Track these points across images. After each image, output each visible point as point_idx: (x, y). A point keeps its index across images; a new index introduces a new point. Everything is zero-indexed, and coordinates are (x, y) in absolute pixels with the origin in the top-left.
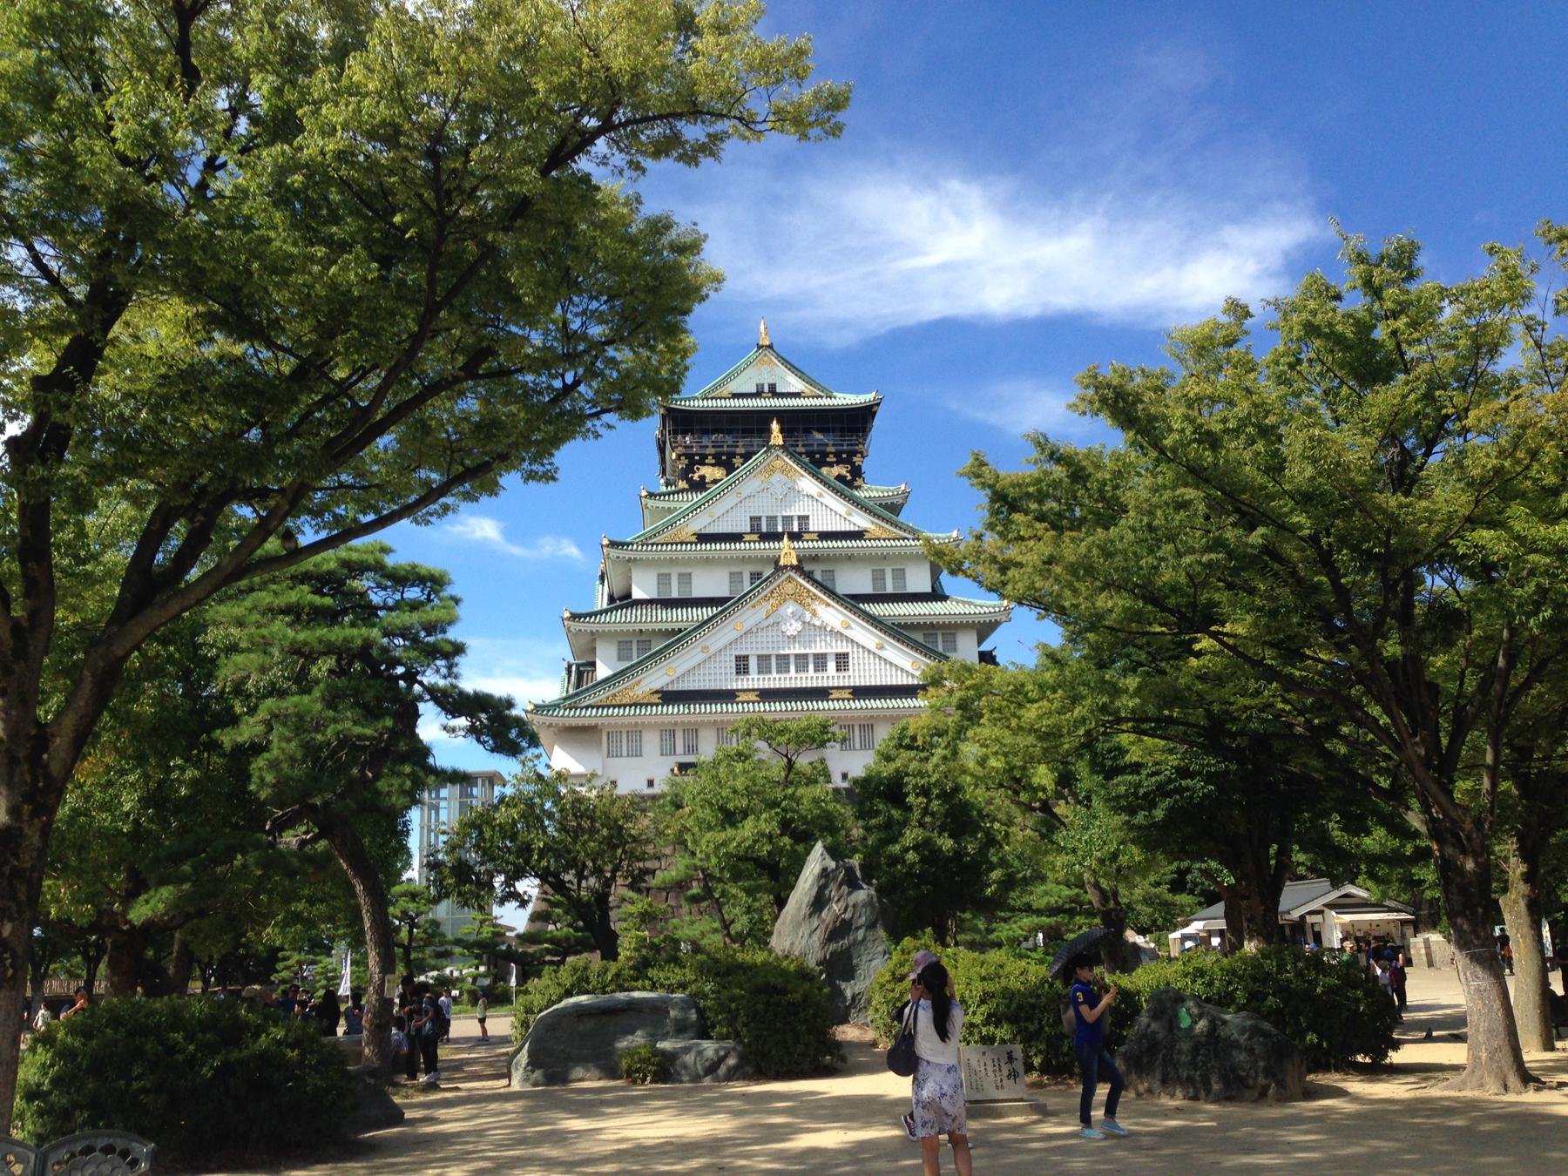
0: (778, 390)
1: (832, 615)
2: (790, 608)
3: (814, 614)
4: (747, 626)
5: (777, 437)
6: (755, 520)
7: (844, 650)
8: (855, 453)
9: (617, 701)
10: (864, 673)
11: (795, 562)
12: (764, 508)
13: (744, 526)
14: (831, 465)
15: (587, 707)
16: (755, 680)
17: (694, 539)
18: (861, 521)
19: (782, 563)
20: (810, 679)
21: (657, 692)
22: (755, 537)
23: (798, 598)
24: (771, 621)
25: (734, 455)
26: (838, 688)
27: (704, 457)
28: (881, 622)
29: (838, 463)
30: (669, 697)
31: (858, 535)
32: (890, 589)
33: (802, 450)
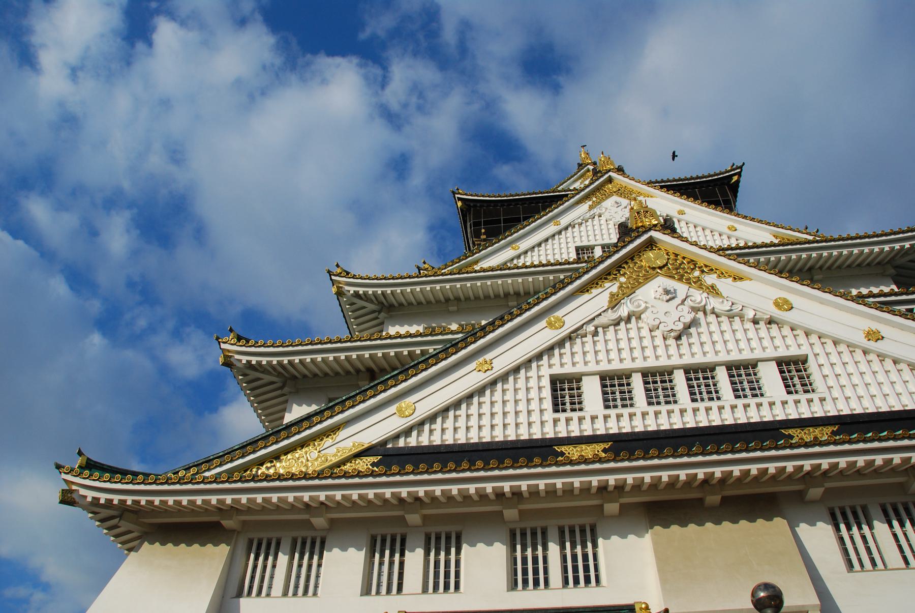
7: (793, 351)
26: (802, 423)
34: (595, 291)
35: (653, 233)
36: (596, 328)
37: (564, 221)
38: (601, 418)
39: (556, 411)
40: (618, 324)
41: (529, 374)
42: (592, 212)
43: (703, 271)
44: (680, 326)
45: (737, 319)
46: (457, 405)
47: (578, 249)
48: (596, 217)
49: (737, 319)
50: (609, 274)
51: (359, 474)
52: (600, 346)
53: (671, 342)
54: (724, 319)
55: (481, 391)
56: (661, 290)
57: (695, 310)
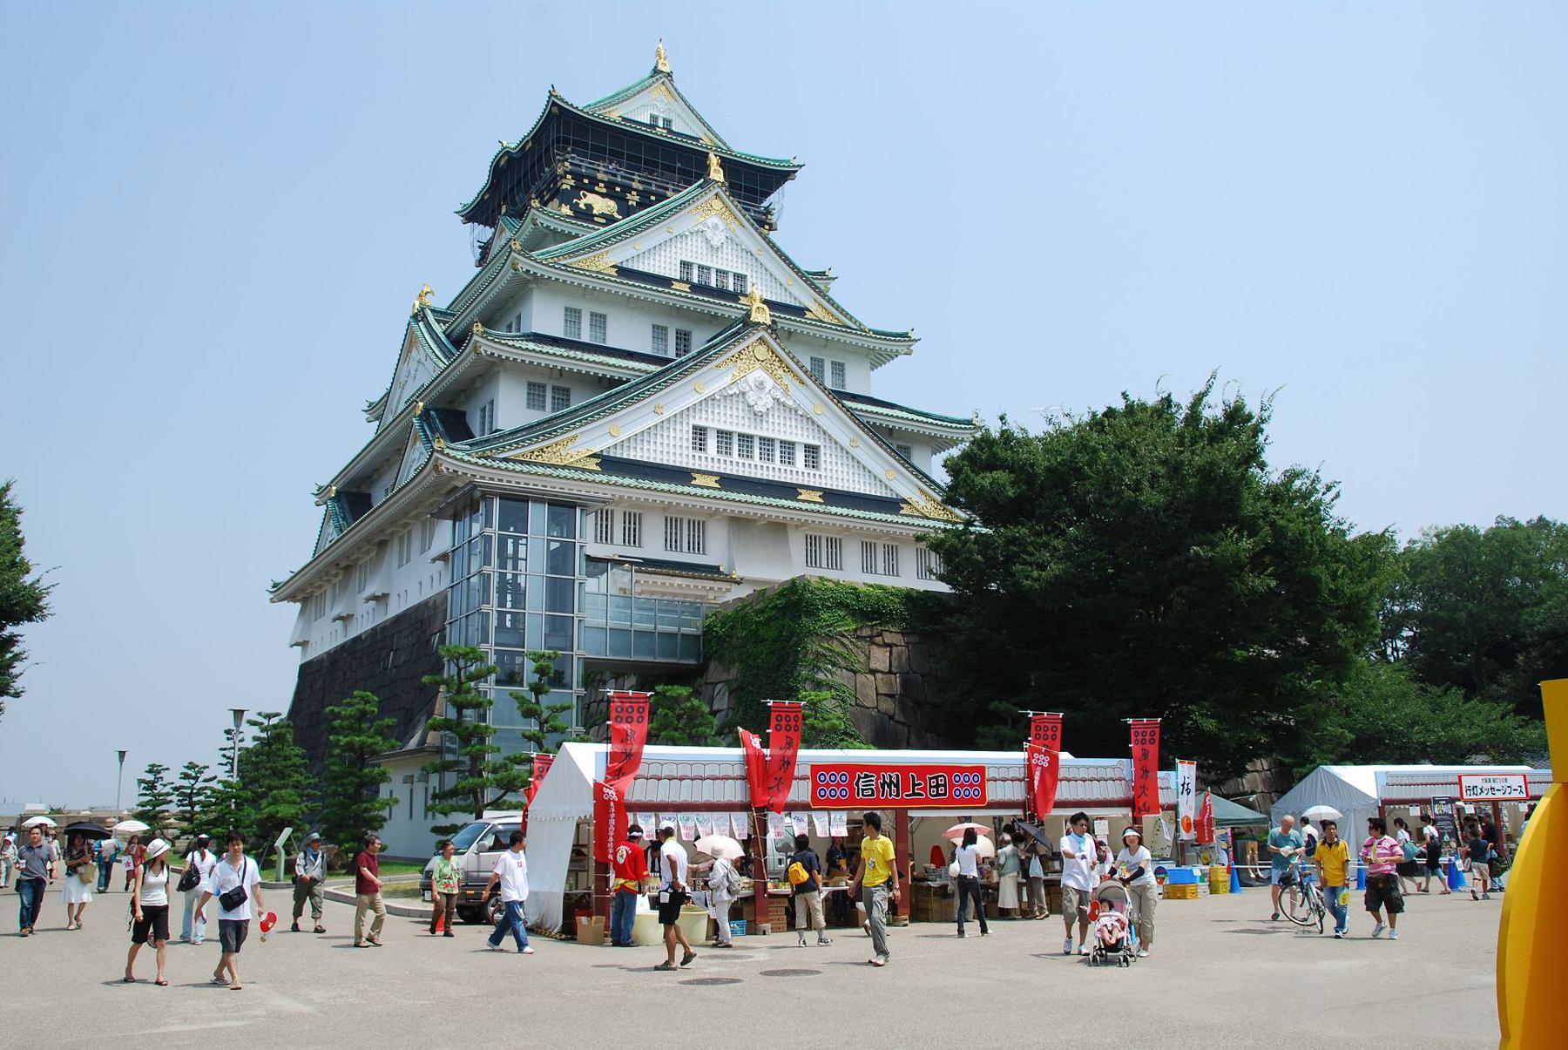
1: (807, 398)
2: (758, 374)
4: (707, 393)
6: (686, 265)
9: (545, 458)
12: (697, 254)
13: (674, 272)
15: (506, 460)
17: (613, 272)
20: (774, 471)
21: (594, 456)
22: (686, 287)
24: (735, 390)
25: (629, 189)
27: (595, 181)
30: (610, 464)
31: (800, 311)
51: (591, 472)
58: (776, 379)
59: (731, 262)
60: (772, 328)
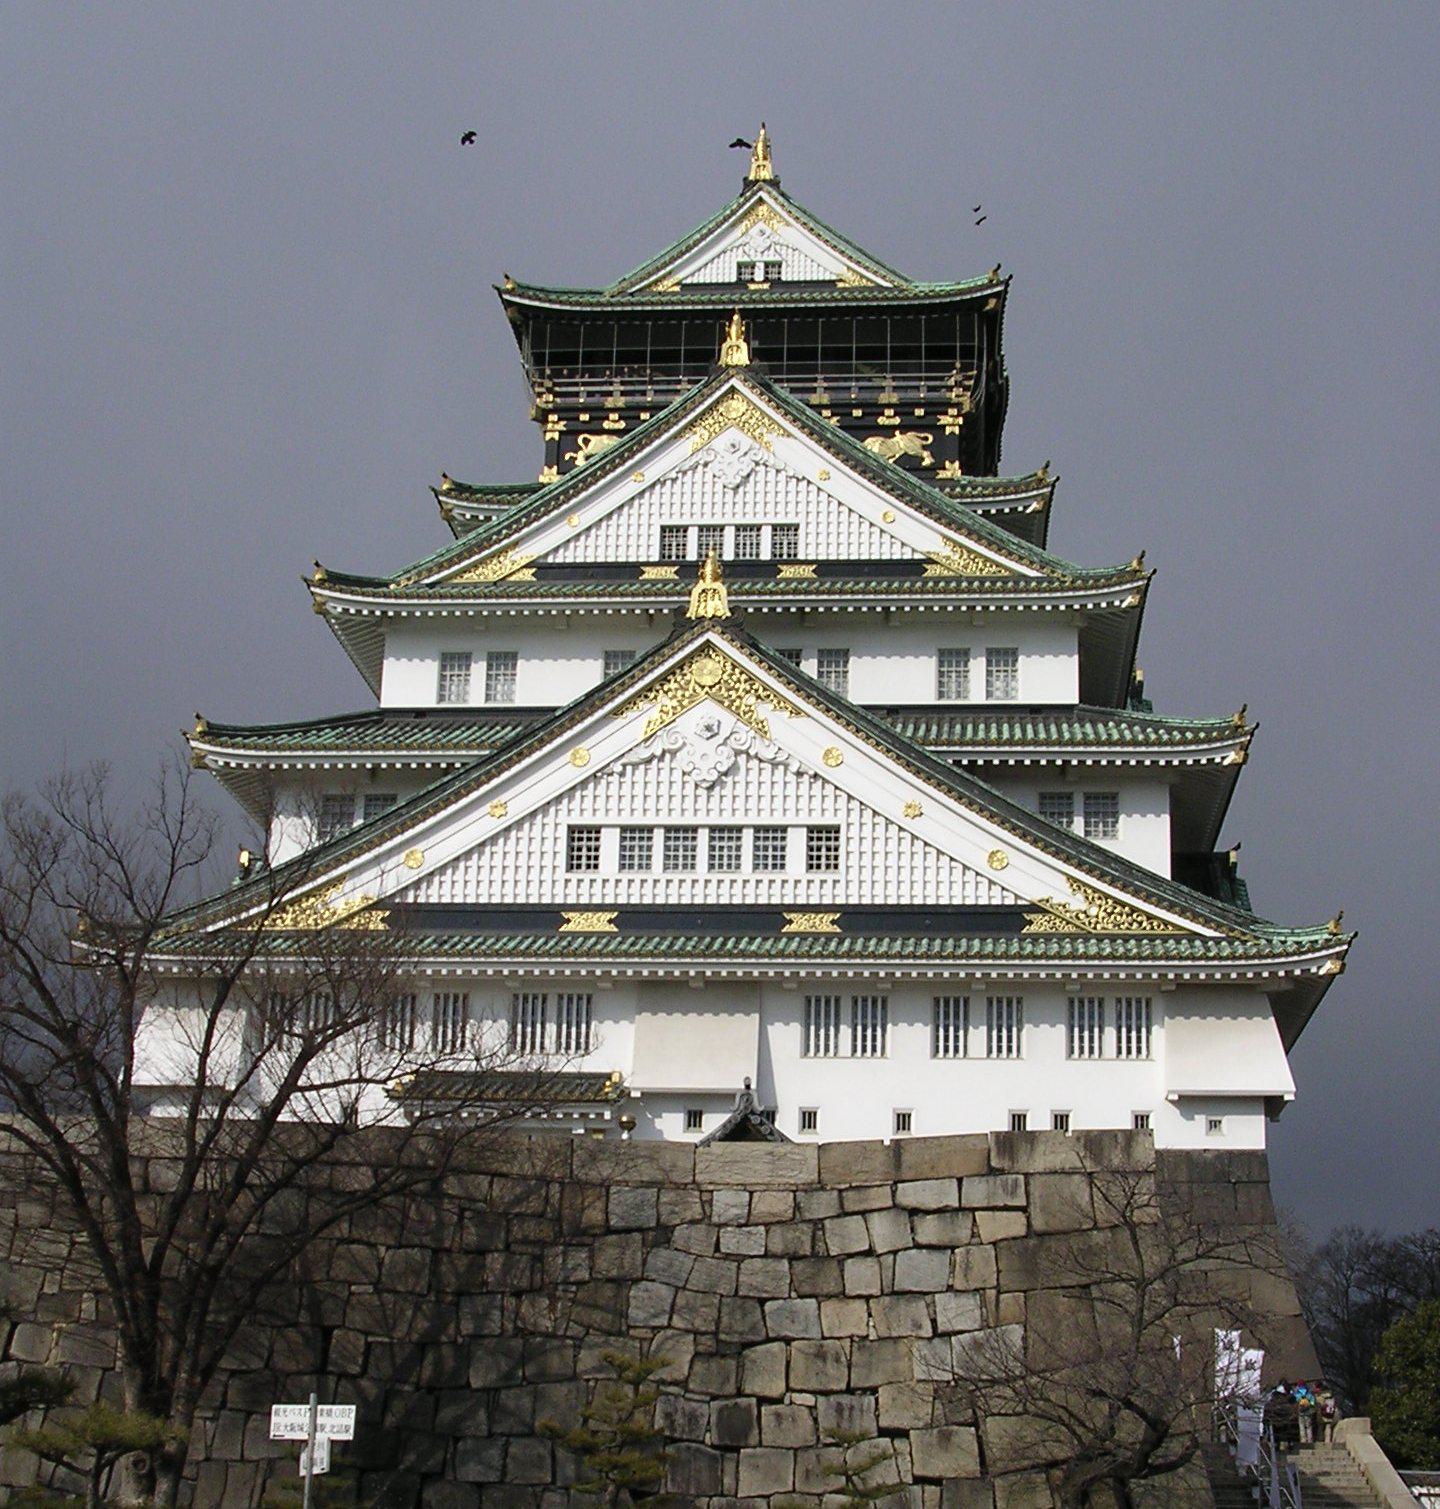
0: (784, 278)
1: (807, 735)
2: (709, 711)
3: (762, 732)
5: (736, 352)
7: (828, 820)
8: (943, 406)
10: (873, 877)
11: (724, 612)
12: (697, 502)
14: (887, 432)
16: (611, 882)
17: (528, 575)
18: (915, 535)
19: (691, 614)
21: (378, 905)
22: (669, 573)
23: (719, 693)
27: (599, 413)
28: (923, 758)
29: (904, 428)
31: (912, 568)
32: (977, 696)
33: (825, 400)
34: (629, 715)
35: (711, 636)
36: (624, 766)
37: (652, 472)
38: (612, 883)
39: (570, 868)
40: (649, 761)
41: (546, 821)
42: (694, 459)
43: (758, 697)
44: (714, 776)
45: (781, 768)
46: (468, 855)
47: (663, 529)
48: (700, 468)
49: (781, 768)
50: (650, 690)
52: (626, 789)
53: (702, 792)
54: (768, 767)
55: (493, 839)
56: (702, 727)
57: (738, 753)
58: (744, 715)
59: (764, 507)
60: (738, 625)
